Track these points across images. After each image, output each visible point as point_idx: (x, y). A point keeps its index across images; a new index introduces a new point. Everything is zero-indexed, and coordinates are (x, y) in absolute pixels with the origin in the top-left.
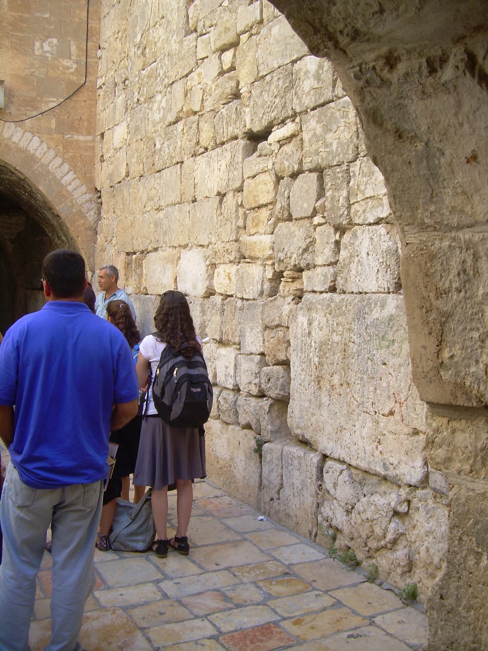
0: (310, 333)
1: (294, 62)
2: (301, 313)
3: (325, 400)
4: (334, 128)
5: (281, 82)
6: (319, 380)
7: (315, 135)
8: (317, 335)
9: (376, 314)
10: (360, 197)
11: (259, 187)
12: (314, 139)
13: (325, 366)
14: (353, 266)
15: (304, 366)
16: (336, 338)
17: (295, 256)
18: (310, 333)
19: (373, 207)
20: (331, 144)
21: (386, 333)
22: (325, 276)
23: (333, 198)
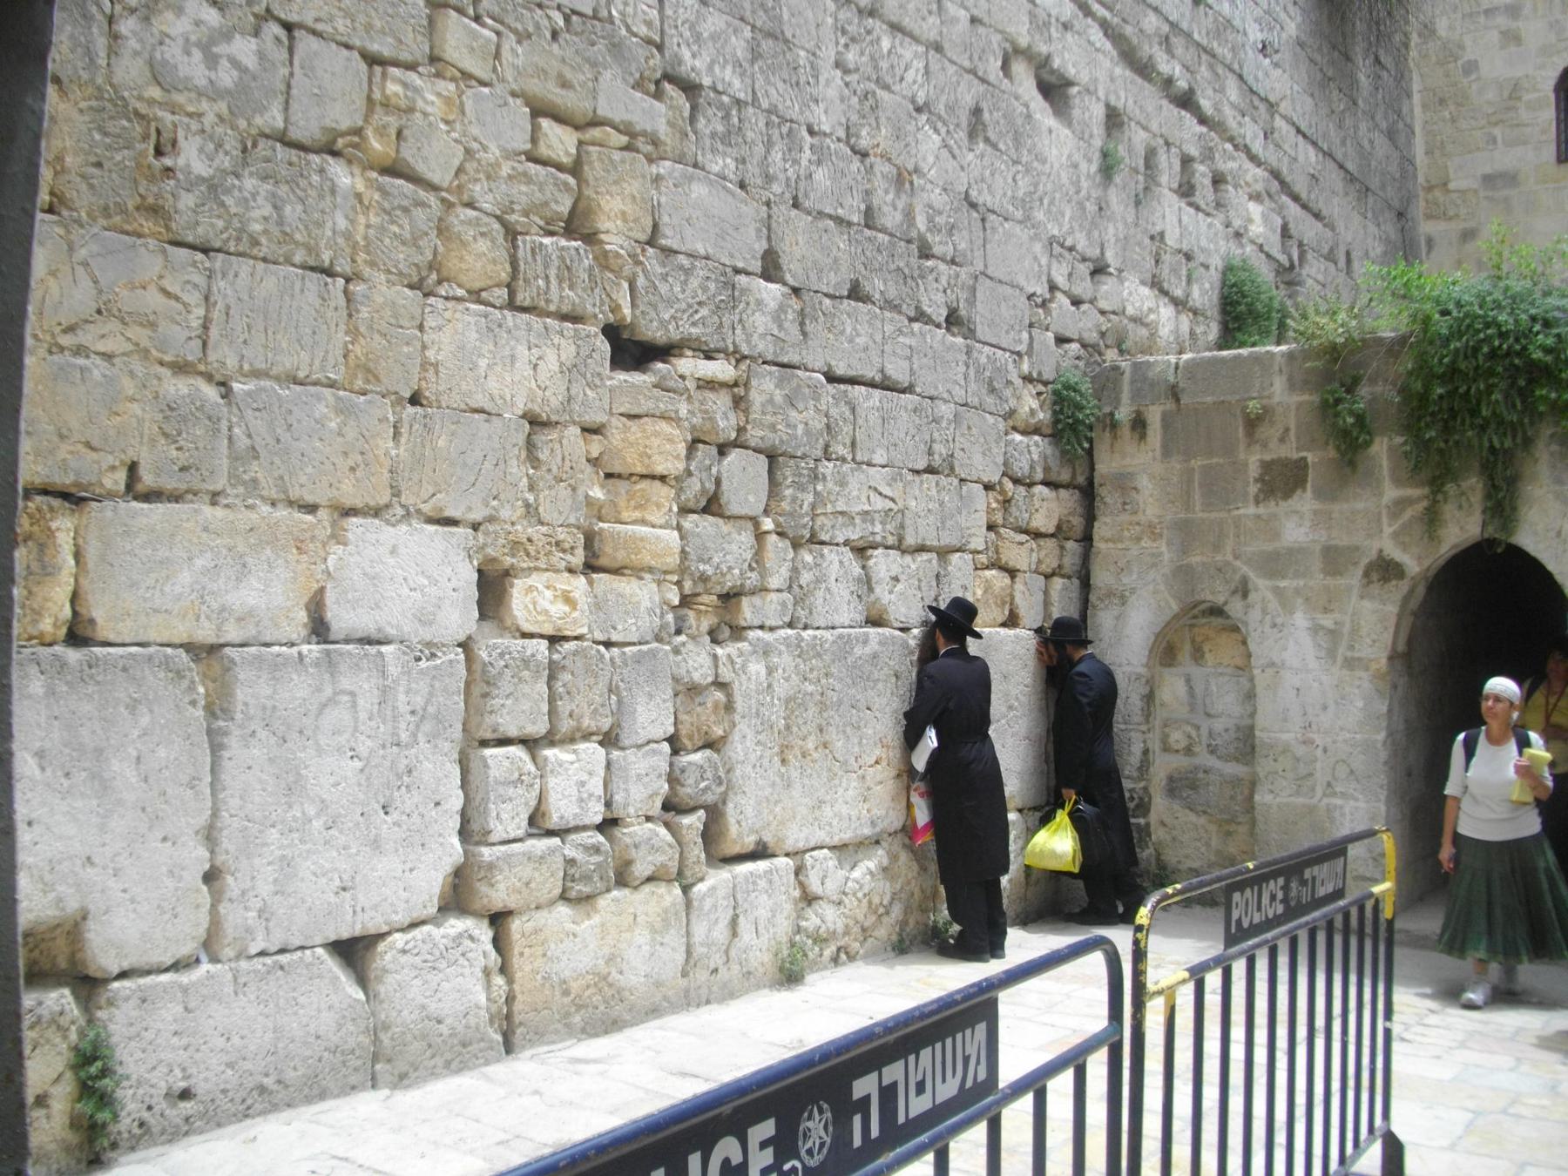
0: (769, 686)
1: (737, 271)
2: (753, 658)
3: (795, 774)
4: (801, 406)
5: (712, 286)
6: (784, 749)
7: (771, 401)
8: (781, 689)
9: (858, 651)
10: (829, 508)
11: (656, 442)
12: (770, 409)
13: (795, 729)
14: (820, 594)
15: (762, 737)
16: (810, 688)
17: (736, 571)
18: (769, 686)
19: (843, 525)
20: (795, 427)
21: (871, 672)
22: (784, 604)
23: (794, 499)
